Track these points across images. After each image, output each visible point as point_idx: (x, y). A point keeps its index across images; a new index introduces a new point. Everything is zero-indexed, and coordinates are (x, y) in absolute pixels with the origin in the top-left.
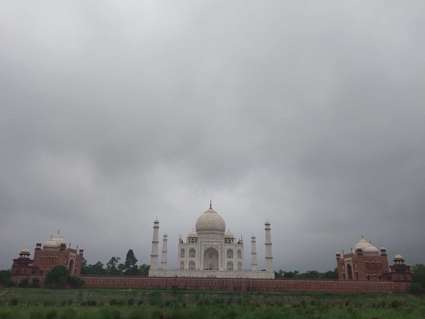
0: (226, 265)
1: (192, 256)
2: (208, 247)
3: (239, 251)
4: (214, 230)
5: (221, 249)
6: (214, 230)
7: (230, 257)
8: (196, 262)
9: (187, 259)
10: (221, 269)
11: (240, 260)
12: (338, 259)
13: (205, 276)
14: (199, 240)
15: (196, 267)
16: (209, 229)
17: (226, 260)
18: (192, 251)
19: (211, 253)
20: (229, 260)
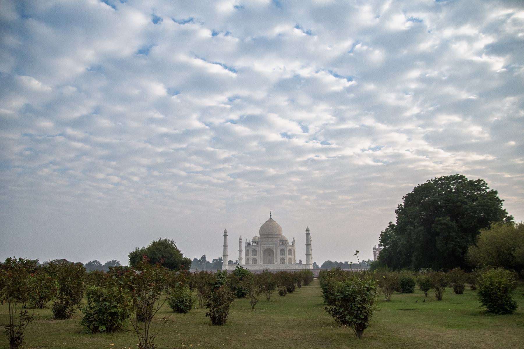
0: (279, 260)
1: (255, 255)
2: (266, 248)
3: (290, 250)
4: (272, 235)
5: (276, 249)
6: (272, 235)
7: (283, 255)
8: (258, 259)
9: (251, 257)
10: (276, 263)
11: (290, 256)
12: (374, 252)
13: (262, 268)
14: (259, 243)
15: (258, 262)
16: (268, 235)
17: (279, 257)
18: (254, 251)
19: (269, 252)
20: (282, 256)
